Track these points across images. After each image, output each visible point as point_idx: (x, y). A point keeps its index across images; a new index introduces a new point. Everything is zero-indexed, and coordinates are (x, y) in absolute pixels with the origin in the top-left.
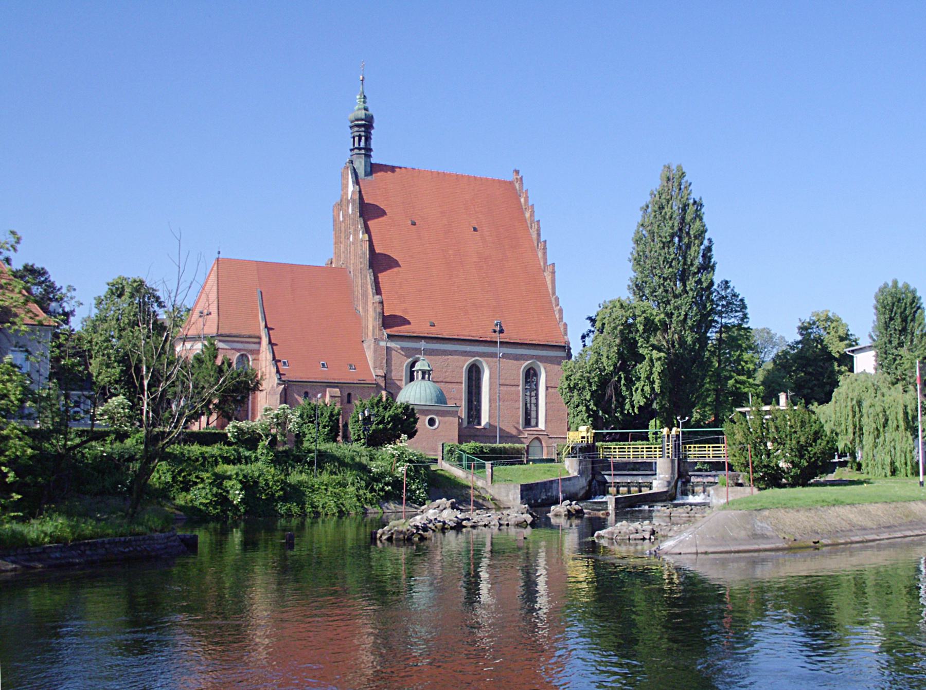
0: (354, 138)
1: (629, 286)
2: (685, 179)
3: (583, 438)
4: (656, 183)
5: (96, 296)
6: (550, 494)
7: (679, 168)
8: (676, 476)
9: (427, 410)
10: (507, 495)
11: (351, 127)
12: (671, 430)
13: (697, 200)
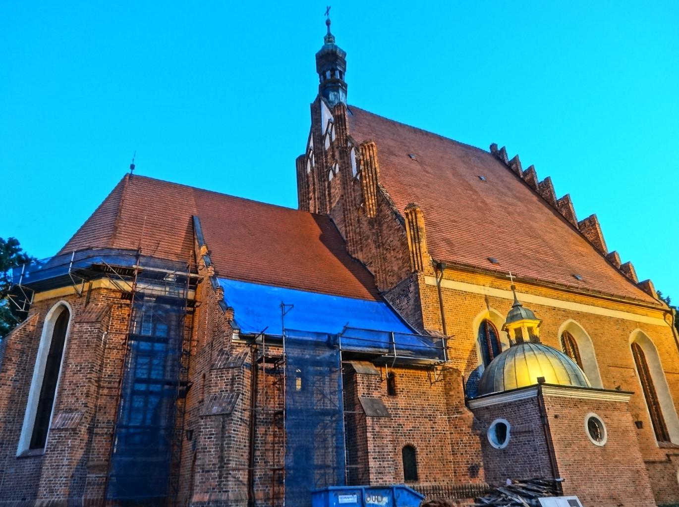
9: (581, 401)
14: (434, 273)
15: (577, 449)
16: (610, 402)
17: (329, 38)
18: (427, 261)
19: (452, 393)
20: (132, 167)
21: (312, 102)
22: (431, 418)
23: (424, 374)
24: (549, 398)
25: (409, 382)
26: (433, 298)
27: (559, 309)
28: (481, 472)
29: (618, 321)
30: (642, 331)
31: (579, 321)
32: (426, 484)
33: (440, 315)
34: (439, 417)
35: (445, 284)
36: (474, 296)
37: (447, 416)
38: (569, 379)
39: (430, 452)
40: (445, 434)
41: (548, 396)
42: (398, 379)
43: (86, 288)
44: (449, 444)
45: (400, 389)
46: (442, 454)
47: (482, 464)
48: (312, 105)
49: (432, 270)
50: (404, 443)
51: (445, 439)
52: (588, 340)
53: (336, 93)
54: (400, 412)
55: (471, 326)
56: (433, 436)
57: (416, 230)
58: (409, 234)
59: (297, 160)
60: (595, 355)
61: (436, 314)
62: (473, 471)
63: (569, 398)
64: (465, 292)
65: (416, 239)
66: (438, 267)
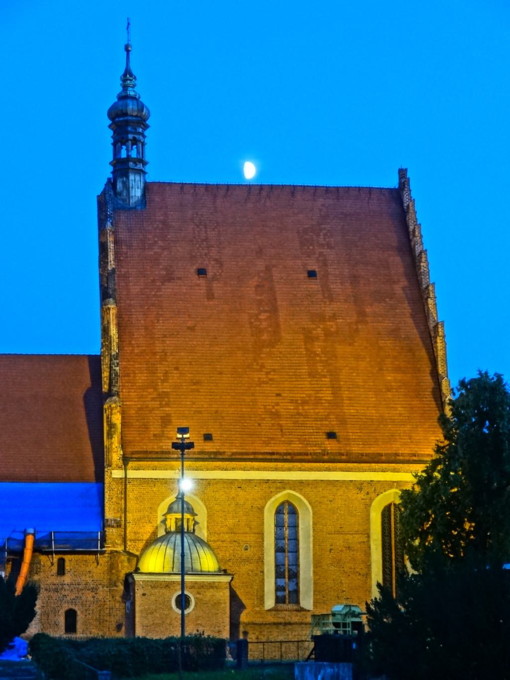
0: (114, 144)
3: (336, 625)
11: (110, 126)
14: (123, 466)
15: (158, 616)
16: (207, 582)
18: (116, 456)
19: (113, 571)
21: (99, 194)
22: (94, 590)
23: (93, 557)
24: (141, 583)
25: (77, 564)
26: (118, 490)
27: (274, 481)
28: (123, 628)
29: (360, 486)
31: (300, 491)
32: (81, 635)
33: (123, 505)
34: (101, 589)
37: (109, 589)
38: (172, 566)
39: (89, 614)
40: (104, 601)
41: (141, 581)
42: (67, 564)
44: (107, 608)
45: (68, 570)
46: (100, 616)
47: (124, 623)
48: (98, 196)
49: (120, 463)
50: (67, 608)
51: (104, 605)
52: (307, 509)
53: (125, 179)
54: (66, 587)
55: (156, 511)
56: (94, 603)
57: (111, 426)
58: (106, 428)
60: (311, 524)
61: (119, 504)
62: (119, 627)
63: (162, 581)
64: (155, 479)
65: (110, 436)
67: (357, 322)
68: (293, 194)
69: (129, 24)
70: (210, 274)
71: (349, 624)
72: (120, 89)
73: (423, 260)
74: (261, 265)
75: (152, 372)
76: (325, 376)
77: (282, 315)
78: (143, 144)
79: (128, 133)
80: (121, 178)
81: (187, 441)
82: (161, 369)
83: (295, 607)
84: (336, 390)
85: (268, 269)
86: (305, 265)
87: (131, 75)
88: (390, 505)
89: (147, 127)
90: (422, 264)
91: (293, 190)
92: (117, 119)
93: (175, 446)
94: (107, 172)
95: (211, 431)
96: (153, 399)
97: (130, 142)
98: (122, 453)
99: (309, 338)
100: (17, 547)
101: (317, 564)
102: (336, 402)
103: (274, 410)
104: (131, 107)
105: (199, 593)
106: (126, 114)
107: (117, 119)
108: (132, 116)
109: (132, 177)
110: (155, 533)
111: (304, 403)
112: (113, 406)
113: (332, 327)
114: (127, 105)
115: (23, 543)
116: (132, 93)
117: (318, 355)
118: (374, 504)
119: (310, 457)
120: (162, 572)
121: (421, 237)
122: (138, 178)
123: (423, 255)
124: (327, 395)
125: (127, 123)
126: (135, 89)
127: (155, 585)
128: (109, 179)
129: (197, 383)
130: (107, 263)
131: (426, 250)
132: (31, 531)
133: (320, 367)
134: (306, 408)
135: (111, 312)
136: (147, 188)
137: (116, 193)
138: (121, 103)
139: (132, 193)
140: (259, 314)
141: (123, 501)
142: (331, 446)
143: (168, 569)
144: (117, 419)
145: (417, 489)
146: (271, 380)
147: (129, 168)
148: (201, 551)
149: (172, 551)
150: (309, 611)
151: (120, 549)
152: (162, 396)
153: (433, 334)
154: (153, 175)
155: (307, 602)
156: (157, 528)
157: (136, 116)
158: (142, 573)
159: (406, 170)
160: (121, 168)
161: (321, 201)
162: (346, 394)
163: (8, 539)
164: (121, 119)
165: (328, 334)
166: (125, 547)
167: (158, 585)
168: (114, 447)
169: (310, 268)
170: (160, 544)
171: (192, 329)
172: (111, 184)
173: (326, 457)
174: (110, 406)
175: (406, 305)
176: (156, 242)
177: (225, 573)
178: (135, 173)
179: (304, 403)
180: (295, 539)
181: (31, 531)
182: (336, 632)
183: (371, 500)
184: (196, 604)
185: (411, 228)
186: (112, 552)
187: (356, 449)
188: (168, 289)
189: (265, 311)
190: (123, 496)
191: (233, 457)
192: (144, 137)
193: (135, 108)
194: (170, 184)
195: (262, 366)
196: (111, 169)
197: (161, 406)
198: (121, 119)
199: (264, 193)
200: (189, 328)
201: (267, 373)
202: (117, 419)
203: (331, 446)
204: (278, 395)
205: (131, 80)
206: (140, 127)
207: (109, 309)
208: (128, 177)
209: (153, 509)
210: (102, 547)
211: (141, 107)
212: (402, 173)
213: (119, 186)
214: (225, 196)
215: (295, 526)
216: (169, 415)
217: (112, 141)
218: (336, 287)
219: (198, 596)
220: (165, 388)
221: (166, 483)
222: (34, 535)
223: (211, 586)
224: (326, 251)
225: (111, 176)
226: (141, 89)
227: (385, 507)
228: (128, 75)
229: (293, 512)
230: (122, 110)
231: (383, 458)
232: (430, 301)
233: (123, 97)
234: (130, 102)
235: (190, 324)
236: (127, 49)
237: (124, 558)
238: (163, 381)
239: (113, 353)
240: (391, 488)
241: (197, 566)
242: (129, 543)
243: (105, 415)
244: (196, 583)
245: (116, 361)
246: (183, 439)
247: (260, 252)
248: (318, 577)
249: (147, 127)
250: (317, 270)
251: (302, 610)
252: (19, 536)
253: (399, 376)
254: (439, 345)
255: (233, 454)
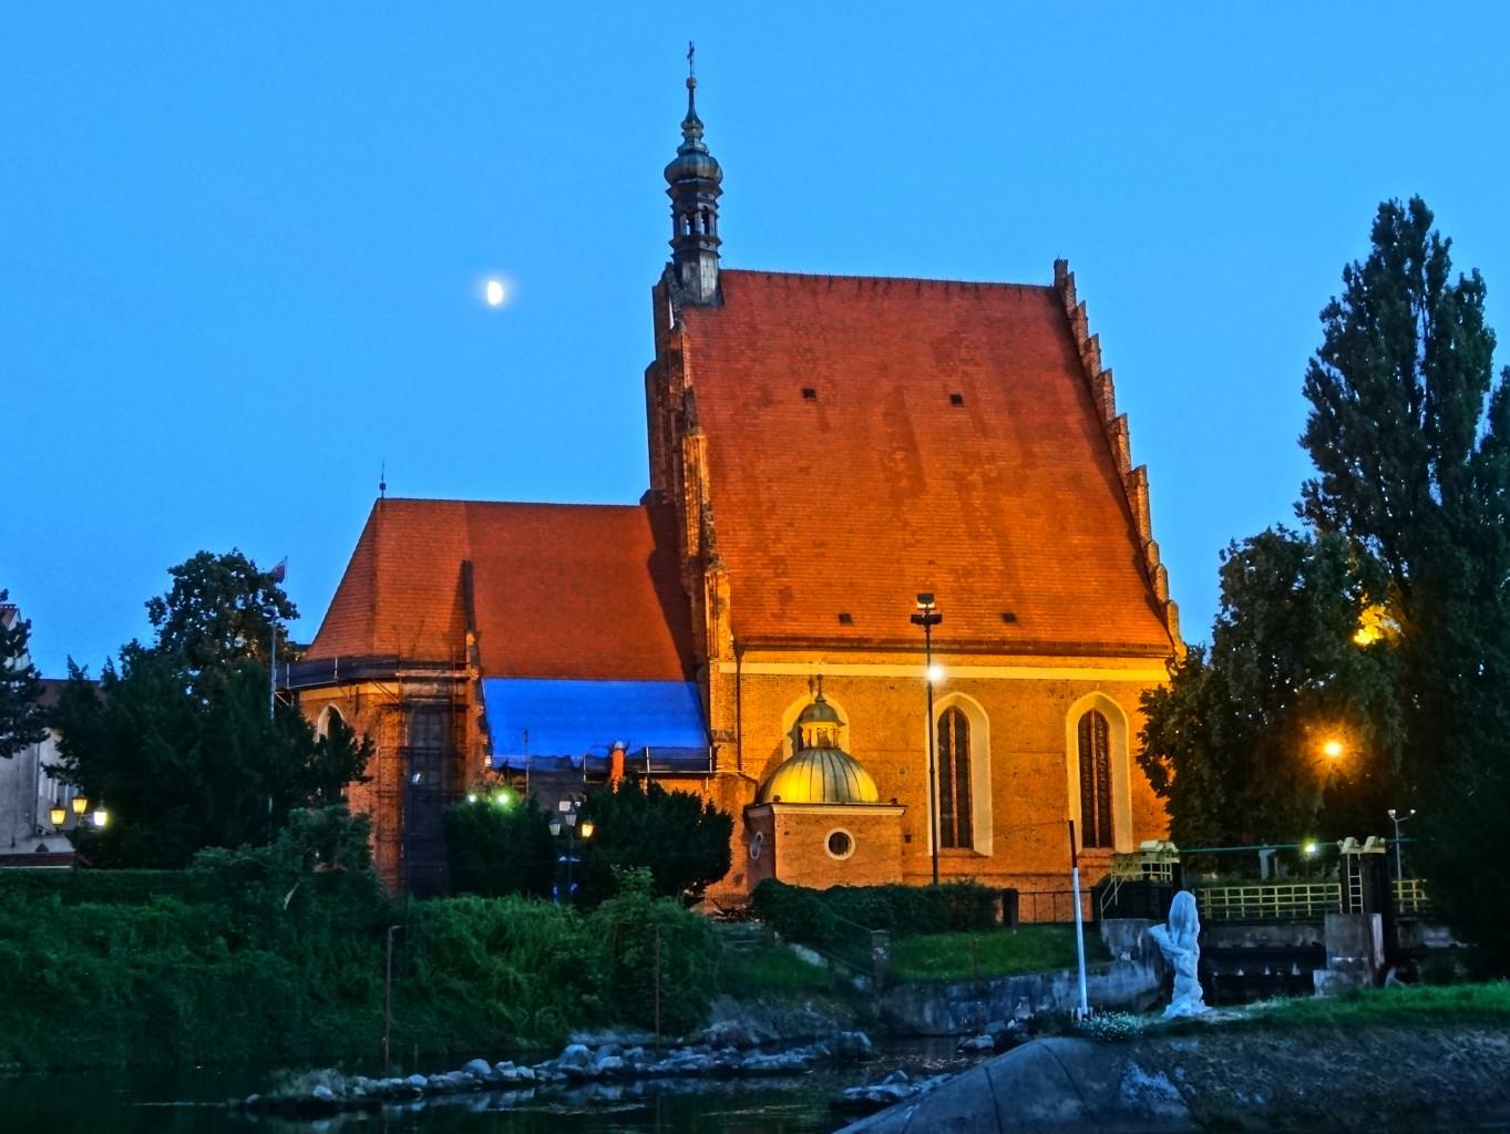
0: (676, 217)
1: (1298, 506)
2: (1431, 230)
3: (1146, 867)
4: (1362, 250)
5: (149, 599)
6: (1044, 1007)
7: (1418, 207)
8: (1380, 959)
9: (827, 817)
10: (920, 1011)
11: (668, 192)
12: (1362, 842)
13: (1469, 277)
17: (691, 124)
18: (723, 639)
20: (383, 487)
21: (656, 284)
26: (728, 689)
28: (745, 881)
29: (1052, 688)
30: (1104, 695)
35: (747, 668)
36: (790, 679)
43: (354, 693)
47: (746, 874)
48: (654, 288)
49: (731, 652)
52: (983, 717)
53: (694, 264)
55: (780, 719)
57: (716, 601)
58: (708, 604)
59: (646, 373)
60: (988, 738)
65: (715, 614)
66: (739, 649)
67: (1023, 466)
68: (918, 290)
69: (692, 51)
70: (821, 395)
71: (1168, 865)
72: (682, 140)
73: (1107, 383)
74: (886, 386)
75: (758, 527)
76: (990, 538)
77: (924, 451)
78: (716, 217)
79: (697, 200)
80: (689, 261)
81: (932, 613)
82: (771, 525)
83: (968, 852)
84: (1007, 557)
85: (898, 390)
86: (945, 387)
87: (698, 121)
88: (1089, 713)
89: (721, 192)
90: (1105, 389)
91: (918, 285)
92: (681, 182)
93: (916, 619)
94: (666, 255)
95: (848, 610)
96: (764, 566)
97: (700, 214)
98: (732, 639)
99: (963, 486)
100: (601, 768)
101: (998, 792)
102: (1008, 574)
103: (928, 583)
104: (702, 165)
105: (860, 831)
106: (694, 175)
107: (681, 182)
108: (702, 177)
109: (703, 262)
110: (779, 751)
111: (968, 573)
112: (720, 573)
113: (990, 470)
114: (695, 163)
115: (609, 762)
116: (699, 146)
117: (976, 509)
118: (1070, 711)
119: (985, 647)
120: (807, 801)
121: (1099, 351)
122: (711, 263)
123: (1106, 376)
124: (995, 563)
125: (696, 186)
126: (703, 140)
127: (801, 820)
128: (668, 264)
129: (822, 544)
130: (683, 378)
131: (1109, 372)
132: (620, 745)
133: (982, 527)
134: (970, 580)
135: (701, 445)
136: (723, 277)
137: (681, 284)
138: (686, 158)
139: (704, 284)
140: (894, 452)
141: (735, 706)
142: (1009, 632)
143: (818, 800)
144: (725, 592)
145: (1170, 689)
146: (919, 541)
147: (700, 250)
148: (858, 774)
149: (820, 774)
150: (987, 857)
151: (734, 771)
152: (777, 562)
153: (1126, 484)
154: (731, 259)
155: (984, 843)
156: (782, 743)
157: (708, 178)
158: (781, 804)
159: (1066, 262)
160: (689, 248)
161: (956, 300)
162: (1020, 562)
163: (587, 757)
164: (688, 181)
165: (987, 481)
166: (740, 768)
167: (805, 819)
168: (721, 629)
169: (954, 391)
170: (800, 764)
171: (805, 470)
172: (674, 270)
173: (1006, 647)
174: (715, 574)
175: (1085, 443)
176: (742, 352)
177: (894, 803)
178: (709, 257)
179: (968, 573)
180: (963, 760)
181: (620, 745)
182: (1147, 876)
183: (1067, 706)
184: (857, 846)
185: (1082, 341)
186: (724, 776)
187: (1044, 635)
188: (766, 417)
189: (899, 448)
190: (735, 698)
191: (884, 646)
192: (717, 207)
193: (707, 166)
194: (752, 273)
195: (906, 523)
196: (672, 251)
197: (777, 576)
198: (688, 181)
199: (880, 289)
200: (801, 470)
201: (913, 533)
202: (725, 592)
203: (1009, 632)
204: (931, 562)
205: (697, 128)
206: (711, 192)
207: (698, 440)
208: (698, 262)
209: (776, 717)
210: (714, 769)
211: (714, 164)
212: (1060, 266)
213: (686, 273)
214: (829, 290)
215: (963, 743)
216: (788, 588)
217: (672, 212)
218: (992, 419)
219: (858, 835)
220: (780, 550)
221: (792, 681)
222: (624, 750)
223: (877, 820)
224: (971, 369)
225: (672, 260)
226: (710, 141)
227: (1082, 720)
228: (691, 124)
229: (962, 724)
230: (688, 169)
231: (1082, 648)
232: (1121, 438)
233: (681, 151)
234: (700, 159)
235: (802, 463)
236: (691, 85)
237: (742, 784)
238: (775, 542)
239: (704, 502)
240: (1093, 689)
241: (856, 795)
242: (744, 764)
243: (706, 587)
244: (856, 817)
245: (709, 513)
246: (927, 610)
247: (884, 369)
248: (998, 811)
249: (721, 192)
250: (963, 394)
251: (979, 856)
252: (603, 753)
253: (1087, 540)
254: (1141, 497)
255: (883, 641)
